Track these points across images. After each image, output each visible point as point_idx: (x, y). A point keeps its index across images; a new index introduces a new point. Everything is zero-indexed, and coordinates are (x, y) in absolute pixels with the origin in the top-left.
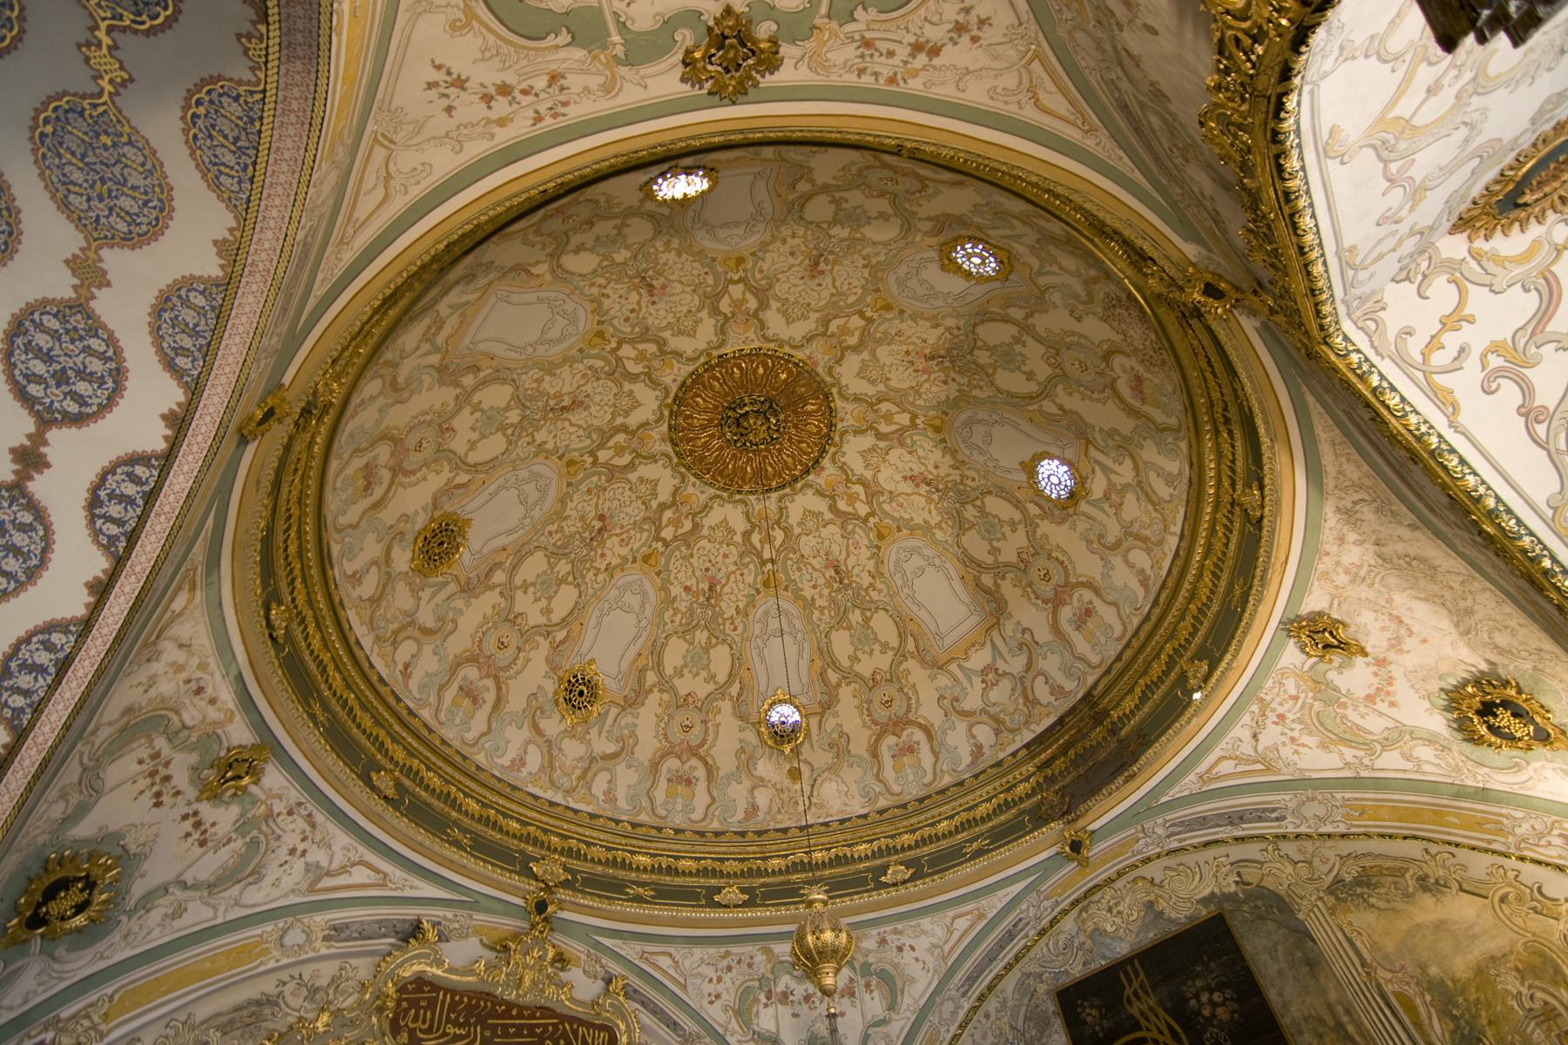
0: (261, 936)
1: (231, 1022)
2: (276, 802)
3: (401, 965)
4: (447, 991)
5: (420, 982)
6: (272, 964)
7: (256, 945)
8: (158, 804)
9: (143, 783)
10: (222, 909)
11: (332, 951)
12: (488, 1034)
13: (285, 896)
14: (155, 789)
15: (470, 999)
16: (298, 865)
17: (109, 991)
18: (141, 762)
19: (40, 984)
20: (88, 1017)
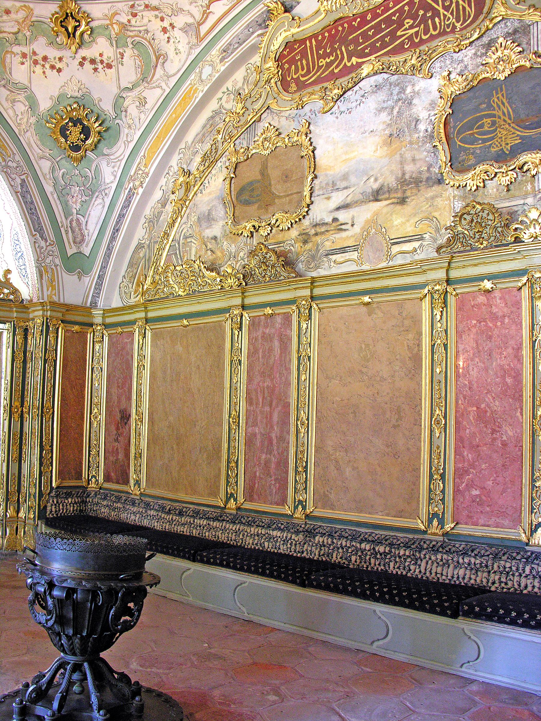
0: (190, 84)
1: (204, 135)
2: (117, 17)
3: (270, 41)
4: (310, 38)
5: (288, 45)
6: (201, 95)
7: (191, 88)
8: (59, 71)
9: (38, 69)
10: (163, 85)
11: (227, 64)
12: (352, 47)
13: (189, 54)
14: (47, 66)
15: (329, 32)
16: (177, 33)
17: (142, 154)
18: (23, 63)
19: (113, 167)
20: (140, 169)
